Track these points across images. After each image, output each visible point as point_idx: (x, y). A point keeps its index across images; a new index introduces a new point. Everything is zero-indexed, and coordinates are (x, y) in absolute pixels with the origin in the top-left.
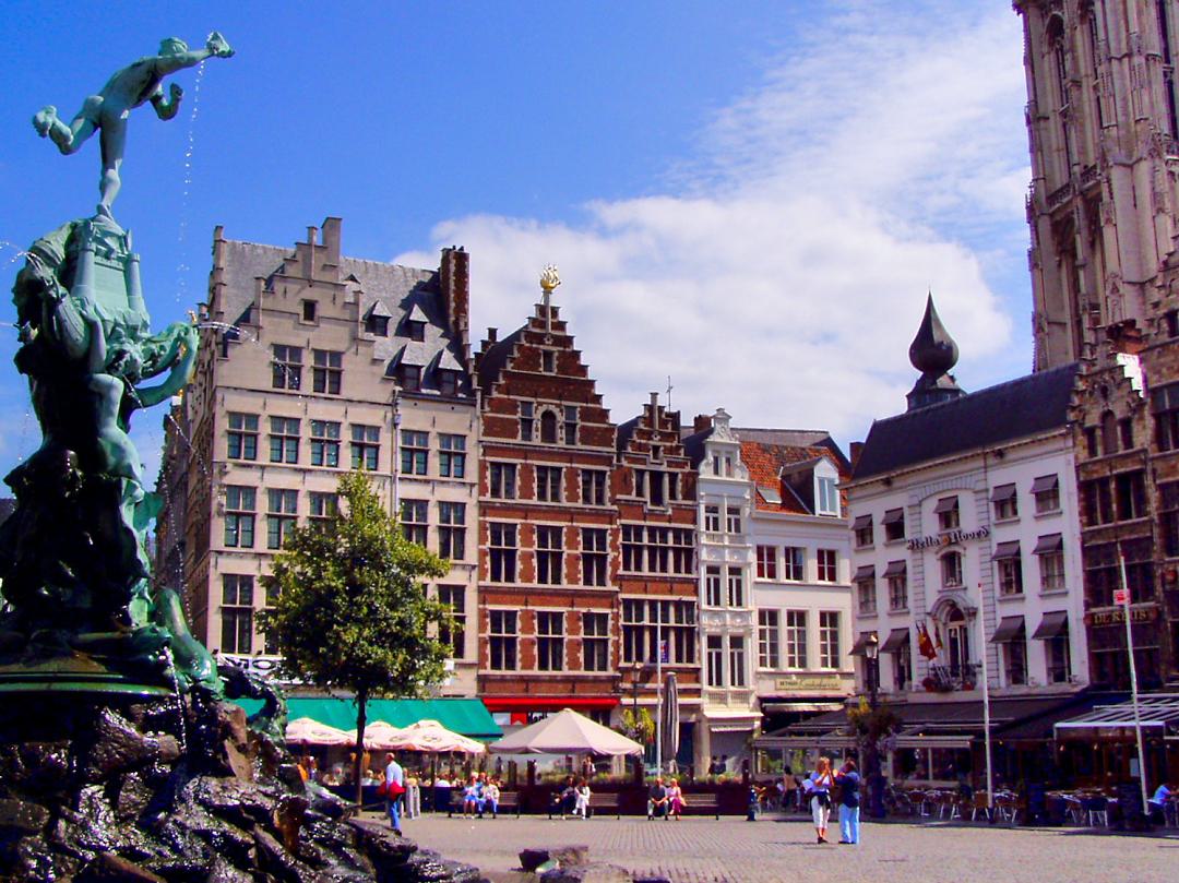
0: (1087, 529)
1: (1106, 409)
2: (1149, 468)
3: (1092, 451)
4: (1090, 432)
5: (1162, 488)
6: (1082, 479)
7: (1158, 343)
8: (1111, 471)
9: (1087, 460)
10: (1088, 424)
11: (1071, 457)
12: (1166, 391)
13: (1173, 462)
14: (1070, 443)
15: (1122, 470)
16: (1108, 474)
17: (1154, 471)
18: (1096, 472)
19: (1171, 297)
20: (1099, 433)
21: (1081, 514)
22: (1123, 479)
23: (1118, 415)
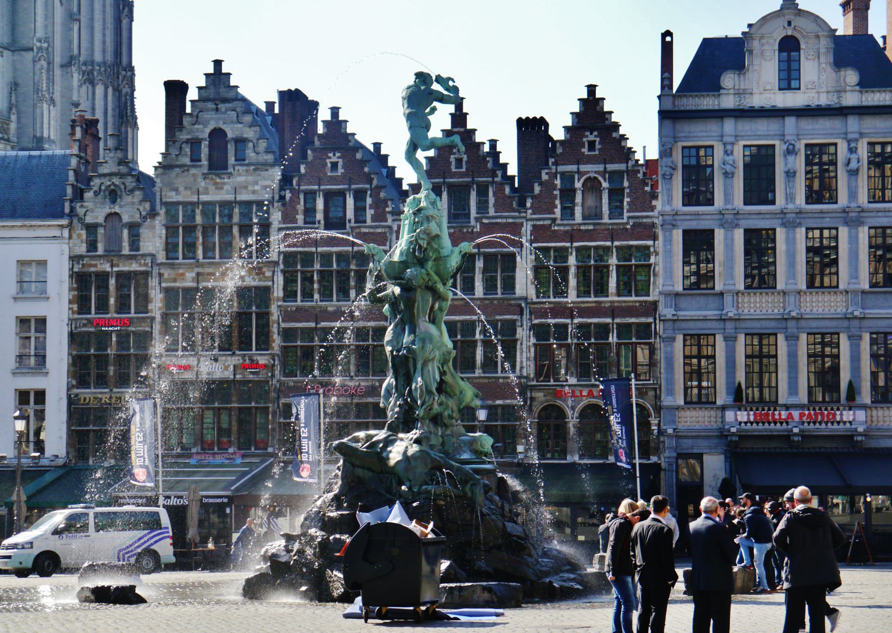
0: (76, 316)
1: (113, 211)
2: (155, 271)
3: (92, 245)
4: (91, 229)
5: (167, 291)
6: (76, 270)
7: (178, 163)
8: (112, 266)
9: (84, 253)
10: (89, 220)
11: (66, 248)
12: (181, 208)
13: (181, 271)
14: (66, 233)
15: (126, 269)
16: (109, 269)
17: (160, 275)
18: (95, 266)
19: (196, 126)
20: (101, 231)
21: (70, 302)
22: (124, 278)
23: (126, 219)
